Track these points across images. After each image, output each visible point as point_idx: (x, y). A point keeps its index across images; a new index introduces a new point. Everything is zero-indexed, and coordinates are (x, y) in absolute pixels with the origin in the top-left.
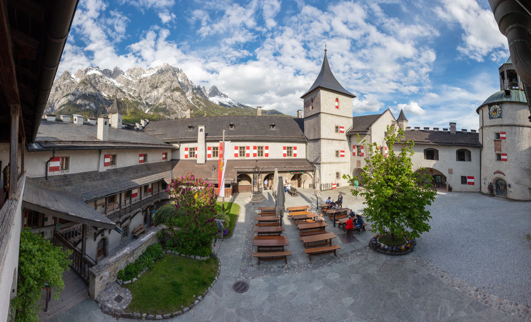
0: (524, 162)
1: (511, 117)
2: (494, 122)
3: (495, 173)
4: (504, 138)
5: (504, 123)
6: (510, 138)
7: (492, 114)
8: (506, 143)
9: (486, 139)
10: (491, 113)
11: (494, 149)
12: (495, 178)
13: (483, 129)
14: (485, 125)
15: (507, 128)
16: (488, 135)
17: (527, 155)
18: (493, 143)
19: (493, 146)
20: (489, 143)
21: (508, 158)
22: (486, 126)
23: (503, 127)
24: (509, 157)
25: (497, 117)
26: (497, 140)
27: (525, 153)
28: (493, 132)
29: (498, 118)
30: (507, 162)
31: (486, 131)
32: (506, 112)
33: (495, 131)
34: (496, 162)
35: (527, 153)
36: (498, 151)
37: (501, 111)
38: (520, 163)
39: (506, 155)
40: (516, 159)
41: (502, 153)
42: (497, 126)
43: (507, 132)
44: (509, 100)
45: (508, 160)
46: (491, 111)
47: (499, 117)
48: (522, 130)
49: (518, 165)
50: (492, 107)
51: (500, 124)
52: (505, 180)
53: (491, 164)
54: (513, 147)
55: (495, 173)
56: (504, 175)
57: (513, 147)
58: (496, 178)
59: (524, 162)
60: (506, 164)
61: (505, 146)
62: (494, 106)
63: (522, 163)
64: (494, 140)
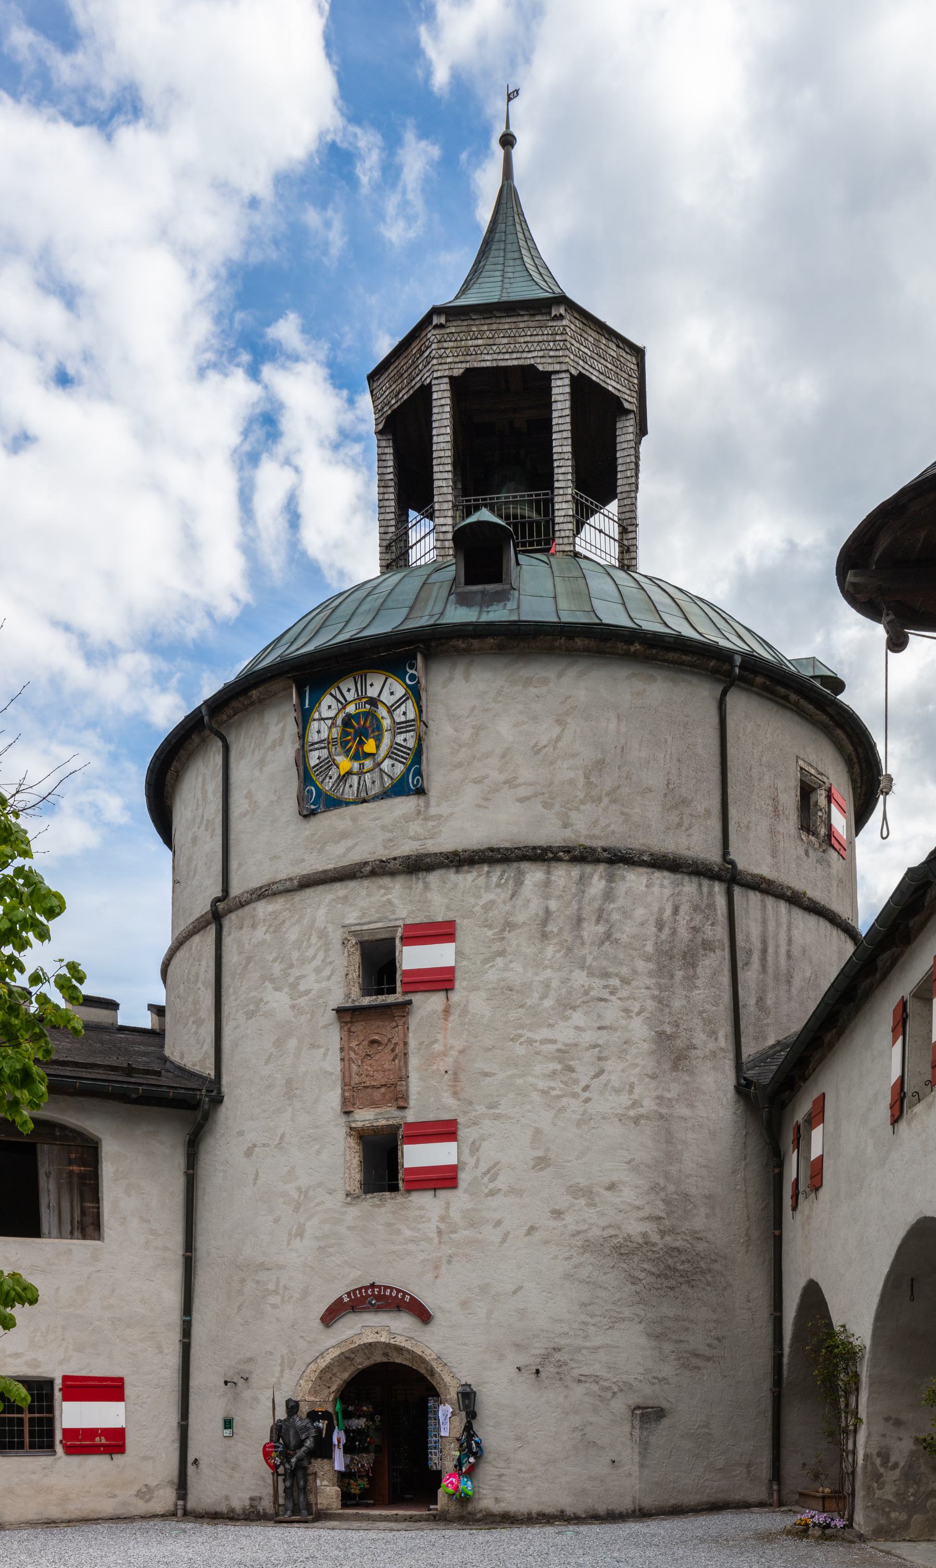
0: (611, 1187)
1: (511, 783)
2: (344, 835)
3: (332, 1315)
6: (492, 976)
8: (454, 1018)
9: (250, 1015)
10: (313, 759)
11: (333, 1097)
12: (335, 1353)
13: (226, 923)
14: (236, 890)
15: (467, 879)
16: (277, 969)
17: (636, 1120)
18: (333, 1037)
19: (333, 1064)
20: (292, 1043)
22: (264, 893)
24: (475, 1148)
25: (376, 790)
26: (366, 1001)
27: (624, 1099)
28: (336, 936)
29: (386, 794)
31: (260, 933)
32: (466, 735)
33: (352, 918)
34: (354, 1212)
35: (635, 1104)
36: (373, 1104)
37: (419, 726)
38: (576, 1191)
40: (541, 1163)
41: (411, 1116)
43: (464, 927)
44: (497, 614)
46: (318, 730)
47: (399, 789)
48: (608, 895)
49: (557, 1214)
50: (327, 700)
51: (407, 848)
52: (429, 1356)
53: (300, 1234)
54: (520, 1050)
55: (332, 1315)
56: (423, 1315)
57: (520, 1050)
58: (345, 1358)
59: (611, 1187)
60: (443, 1219)
61: (444, 1054)
63: (587, 1193)
64: (340, 1011)
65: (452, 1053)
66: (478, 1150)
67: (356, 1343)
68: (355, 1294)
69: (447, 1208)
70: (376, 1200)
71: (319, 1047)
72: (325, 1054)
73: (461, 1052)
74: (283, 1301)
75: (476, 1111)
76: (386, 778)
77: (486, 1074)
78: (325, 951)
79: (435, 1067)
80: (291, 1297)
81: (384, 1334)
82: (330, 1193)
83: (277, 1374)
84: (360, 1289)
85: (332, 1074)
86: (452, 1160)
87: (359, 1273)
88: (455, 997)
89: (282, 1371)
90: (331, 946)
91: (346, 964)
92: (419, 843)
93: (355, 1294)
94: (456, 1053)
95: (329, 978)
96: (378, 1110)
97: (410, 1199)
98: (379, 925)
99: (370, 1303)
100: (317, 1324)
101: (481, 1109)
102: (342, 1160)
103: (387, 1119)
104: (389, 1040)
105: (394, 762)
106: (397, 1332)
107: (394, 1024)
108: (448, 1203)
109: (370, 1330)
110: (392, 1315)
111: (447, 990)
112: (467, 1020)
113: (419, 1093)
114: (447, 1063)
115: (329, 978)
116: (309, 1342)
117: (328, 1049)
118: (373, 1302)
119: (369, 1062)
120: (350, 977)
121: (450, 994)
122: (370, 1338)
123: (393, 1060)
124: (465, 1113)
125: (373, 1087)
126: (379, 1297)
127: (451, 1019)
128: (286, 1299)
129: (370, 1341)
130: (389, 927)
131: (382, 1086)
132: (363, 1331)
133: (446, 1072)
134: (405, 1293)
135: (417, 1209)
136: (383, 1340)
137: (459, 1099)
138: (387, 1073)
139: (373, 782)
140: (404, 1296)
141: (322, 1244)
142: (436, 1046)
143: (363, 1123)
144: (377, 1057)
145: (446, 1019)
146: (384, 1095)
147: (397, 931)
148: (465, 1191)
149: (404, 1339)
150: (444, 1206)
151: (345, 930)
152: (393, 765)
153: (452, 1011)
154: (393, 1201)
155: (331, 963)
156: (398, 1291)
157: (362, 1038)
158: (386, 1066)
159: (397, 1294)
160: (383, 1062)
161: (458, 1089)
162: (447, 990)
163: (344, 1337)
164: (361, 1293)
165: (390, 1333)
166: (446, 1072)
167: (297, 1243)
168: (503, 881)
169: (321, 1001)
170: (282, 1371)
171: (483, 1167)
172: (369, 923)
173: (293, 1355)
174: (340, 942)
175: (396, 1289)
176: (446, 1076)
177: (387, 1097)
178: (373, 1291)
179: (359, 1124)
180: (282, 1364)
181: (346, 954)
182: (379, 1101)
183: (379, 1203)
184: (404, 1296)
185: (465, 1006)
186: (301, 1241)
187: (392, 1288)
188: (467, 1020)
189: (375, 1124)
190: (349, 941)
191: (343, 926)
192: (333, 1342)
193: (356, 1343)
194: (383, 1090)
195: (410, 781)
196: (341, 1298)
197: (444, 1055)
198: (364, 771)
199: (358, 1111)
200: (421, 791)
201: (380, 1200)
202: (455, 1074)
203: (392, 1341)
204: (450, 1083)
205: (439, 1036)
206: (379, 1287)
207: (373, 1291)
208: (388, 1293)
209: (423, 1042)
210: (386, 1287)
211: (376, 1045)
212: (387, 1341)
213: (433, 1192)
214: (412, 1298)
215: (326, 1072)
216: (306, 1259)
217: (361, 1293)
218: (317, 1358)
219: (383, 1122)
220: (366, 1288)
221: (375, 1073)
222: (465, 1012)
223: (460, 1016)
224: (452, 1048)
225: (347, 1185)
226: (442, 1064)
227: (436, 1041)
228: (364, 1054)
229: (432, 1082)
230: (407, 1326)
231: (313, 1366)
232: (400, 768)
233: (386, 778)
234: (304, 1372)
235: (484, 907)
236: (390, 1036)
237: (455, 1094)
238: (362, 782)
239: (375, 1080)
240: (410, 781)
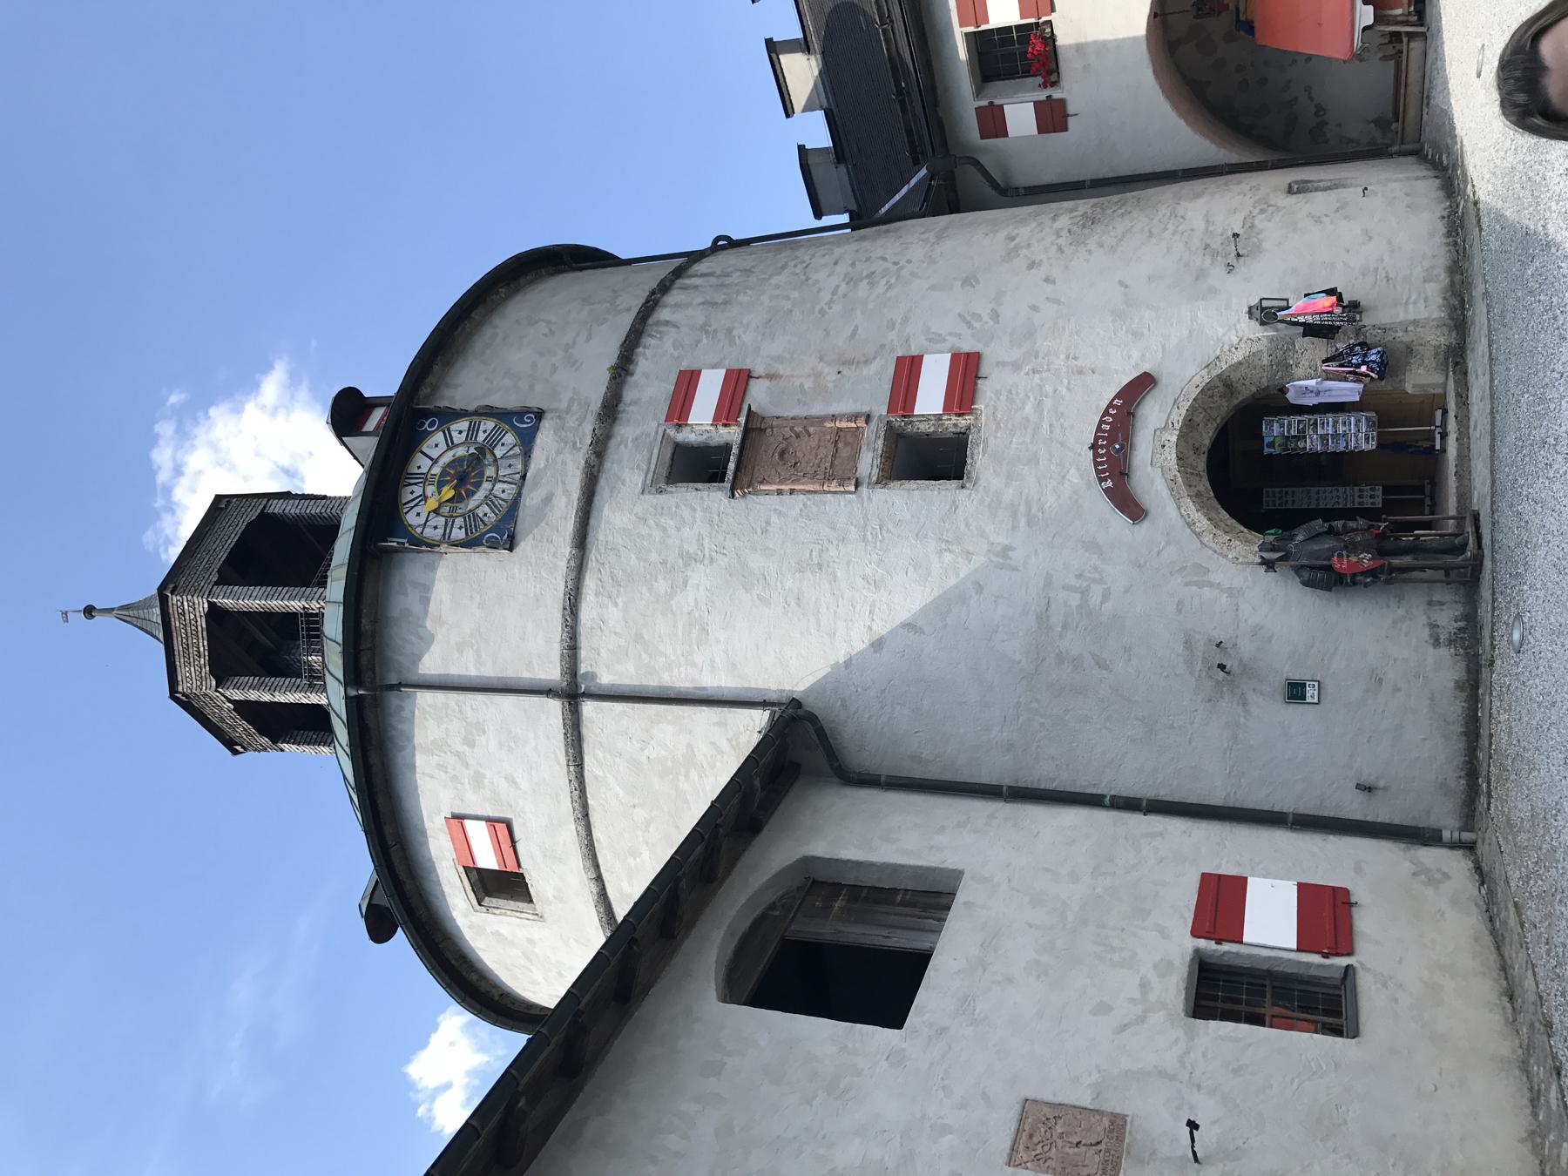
3: (1129, 505)
4: (737, 382)
5: (595, 389)
7: (472, 518)
21: (952, 342)
23: (629, 395)
25: (518, 466)
29: (527, 455)
30: (994, 354)
36: (855, 457)
39: (908, 371)
41: (881, 409)
42: (600, 448)
43: (686, 365)
45: (968, 346)
47: (527, 441)
55: (1129, 505)
56: (1143, 384)
61: (818, 376)
62: (406, 495)
65: (819, 368)
66: (940, 335)
67: (1175, 476)
68: (1103, 471)
69: (1004, 364)
72: (780, 514)
74: (1100, 581)
75: (892, 341)
76: (511, 453)
77: (854, 333)
79: (831, 385)
80: (1095, 568)
81: (1166, 436)
83: (1216, 592)
84: (1096, 464)
86: (946, 359)
87: (1073, 471)
88: (759, 369)
89: (1211, 585)
92: (589, 415)
93: (1103, 471)
94: (821, 364)
96: (864, 448)
98: (656, 452)
99: (1118, 451)
100: (1143, 529)
101: (893, 336)
102: (916, 492)
103: (877, 437)
105: (500, 443)
106: (1165, 418)
108: (998, 363)
109: (1159, 456)
110: (1139, 424)
111: (750, 377)
114: (829, 373)
116: (1168, 543)
118: (1117, 446)
119: (804, 465)
121: (755, 374)
122: (1171, 456)
124: (892, 350)
126: (1111, 439)
127: (781, 373)
128: (1097, 576)
129: (1174, 456)
130: (661, 442)
132: (1158, 465)
133: (839, 372)
134: (1111, 405)
136: (1174, 439)
137: (875, 358)
139: (510, 466)
140: (1115, 407)
141: (1023, 521)
142: (806, 387)
144: (800, 454)
145: (781, 377)
146: (846, 444)
147: (669, 436)
148: (987, 345)
149: (1175, 411)
150: (1001, 367)
151: (646, 491)
152: (503, 444)
156: (1106, 413)
157: (773, 472)
158: (814, 444)
159: (1111, 415)
161: (862, 359)
162: (750, 377)
163: (1165, 492)
164: (1102, 463)
165: (1165, 428)
166: (839, 372)
167: (1016, 556)
168: (658, 336)
170: (1211, 585)
171: (963, 329)
173: (1185, 568)
175: (1103, 416)
176: (844, 372)
177: (851, 440)
178: (1102, 447)
179: (875, 471)
180: (1200, 585)
182: (852, 449)
184: (1115, 407)
186: (1015, 549)
187: (1101, 422)
191: (643, 493)
192: (1171, 507)
193: (1175, 476)
194: (840, 445)
195: (525, 426)
196: (1106, 491)
198: (495, 476)
200: (540, 415)
202: (844, 364)
203: (1177, 426)
205: (797, 383)
206: (1097, 438)
207: (1102, 447)
208: (1107, 427)
210: (1099, 429)
212: (1177, 433)
214: (1118, 396)
216: (1042, 543)
217: (1102, 463)
218: (1194, 532)
219: (880, 442)
220: (1096, 455)
222: (779, 359)
226: (828, 378)
227: (802, 386)
229: (847, 387)
230: (1157, 407)
231: (1207, 539)
232: (510, 438)
233: (511, 453)
234: (1215, 552)
237: (866, 362)
238: (505, 479)
239: (826, 456)
240: (525, 426)
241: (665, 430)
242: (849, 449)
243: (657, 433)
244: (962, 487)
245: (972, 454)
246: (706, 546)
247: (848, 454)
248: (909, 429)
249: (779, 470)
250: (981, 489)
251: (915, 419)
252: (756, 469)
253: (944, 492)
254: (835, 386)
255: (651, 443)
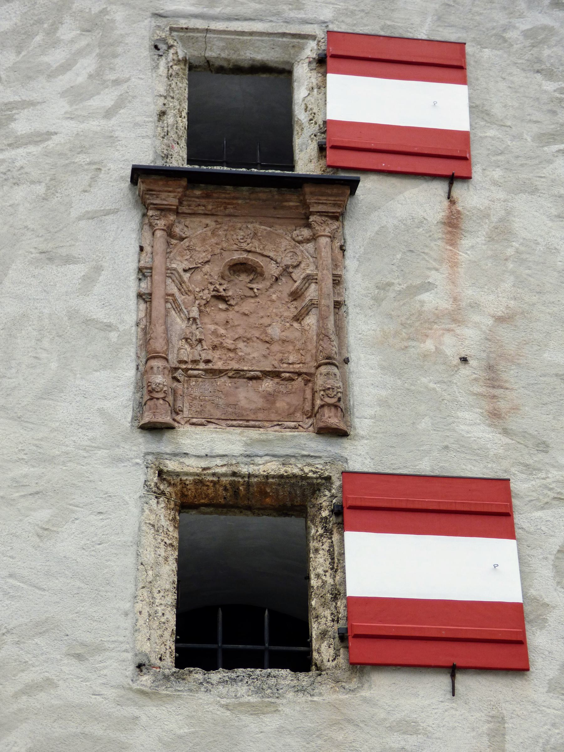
65: (476, 318)
70: (242, 689)
71: (69, 260)
73: (500, 320)
78: (101, 56)
79: (429, 345)
82: (79, 657)
85: (109, 327)
90: (120, 50)
91: (162, 90)
94: (490, 322)
95: (109, 114)
96: (254, 434)
97: (365, 693)
102: (130, 560)
103: (285, 459)
104: (287, 271)
107: (306, 233)
111: (451, 179)
112: (510, 252)
113: (383, 403)
115: (109, 114)
117: (98, 269)
119: (222, 316)
120: (170, 119)
121: (459, 190)
123: (298, 318)
125: (238, 374)
127: (466, 242)
130: (284, 35)
131: (266, 374)
135: (391, 729)
137: (506, 432)
138: (275, 348)
142: (426, 297)
143: (204, 463)
144: (248, 306)
146: (270, 398)
147: (302, 48)
151: (162, 22)
153: (466, 225)
154: (302, 698)
155: (117, 82)
158: (275, 331)
160: (266, 321)
161: (503, 405)
166: (464, 360)
169: (82, 159)
172: (229, 19)
174: (147, 44)
176: (465, 371)
177: (281, 404)
181: (162, 69)
183: (254, 699)
185: (501, 220)
188: (510, 252)
189: (244, 470)
190: (170, 47)
194: (268, 385)
197: (455, 321)
199: (188, 428)
201: (259, 690)
204: (477, 389)
205: (435, 277)
209: (390, 284)
211: (244, 278)
213: (444, 681)
215: (88, 322)
221: (241, 345)
223: (491, 239)
224: (475, 306)
225: (141, 637)
226: (448, 339)
227: (427, 287)
228: (206, 295)
235: (527, 34)
236: (288, 261)
241: (314, 37)
242: (260, 402)
243: (305, 22)
244: (140, 666)
245: (234, 680)
246: (21, 151)
247: (243, 403)
248: (315, 530)
249: (207, 268)
250: (131, 711)
251: (336, 537)
252: (208, 221)
253: (127, 623)
254: (425, 356)
255: (278, 14)
